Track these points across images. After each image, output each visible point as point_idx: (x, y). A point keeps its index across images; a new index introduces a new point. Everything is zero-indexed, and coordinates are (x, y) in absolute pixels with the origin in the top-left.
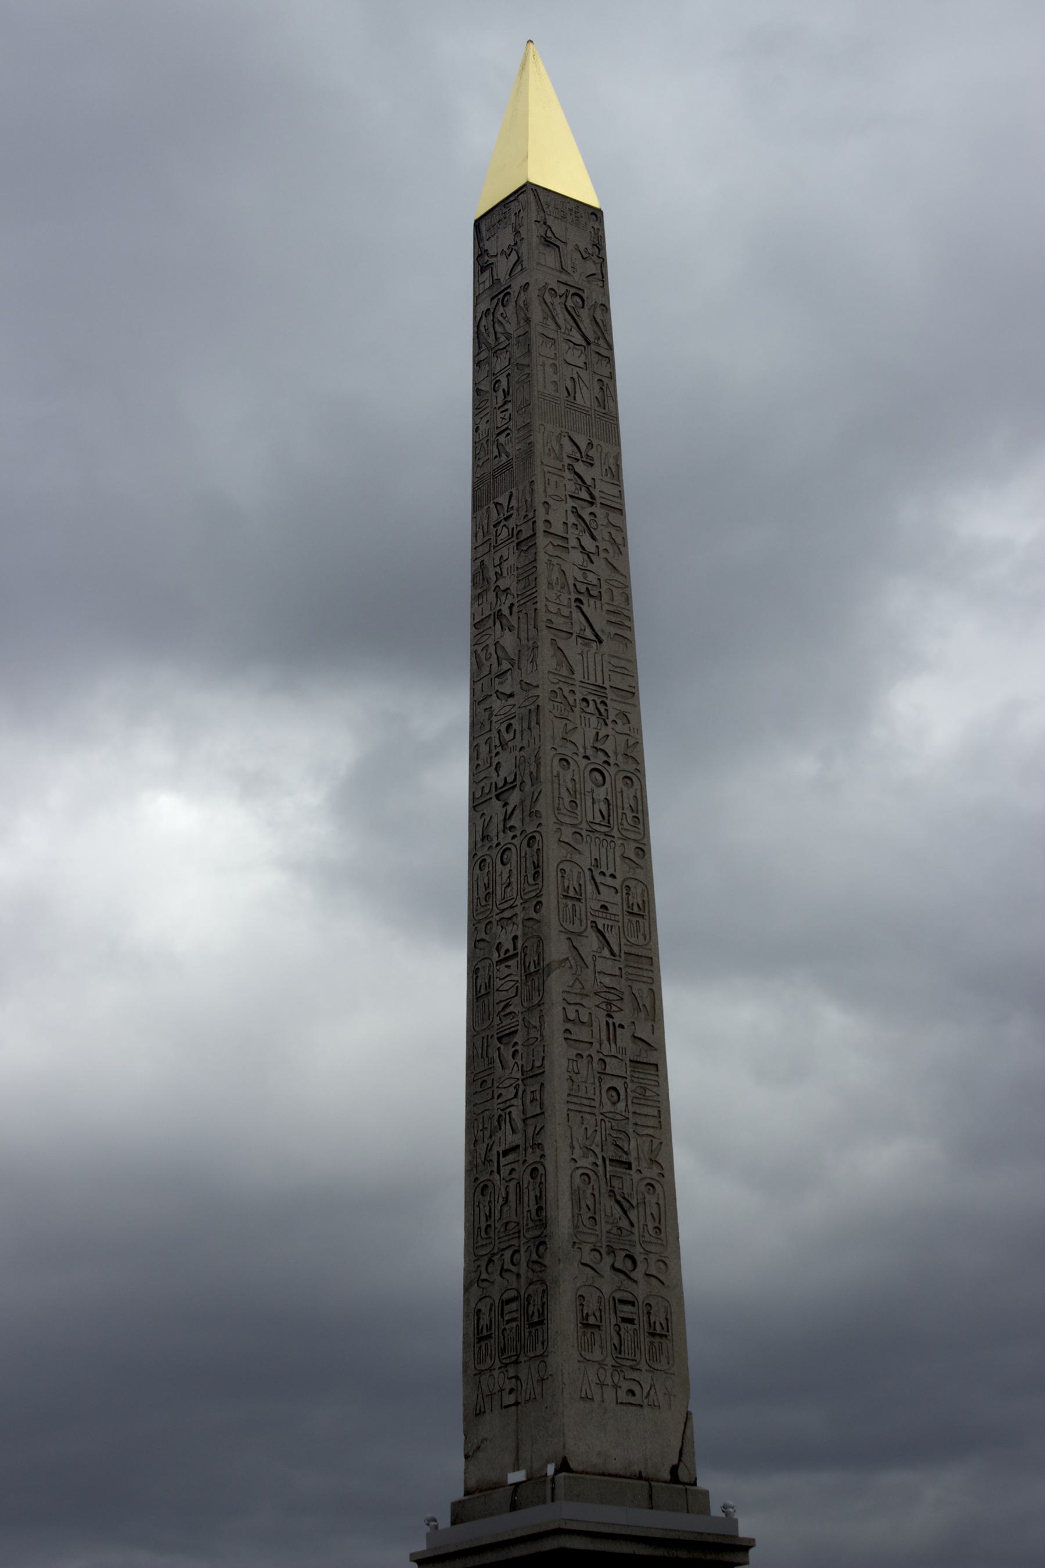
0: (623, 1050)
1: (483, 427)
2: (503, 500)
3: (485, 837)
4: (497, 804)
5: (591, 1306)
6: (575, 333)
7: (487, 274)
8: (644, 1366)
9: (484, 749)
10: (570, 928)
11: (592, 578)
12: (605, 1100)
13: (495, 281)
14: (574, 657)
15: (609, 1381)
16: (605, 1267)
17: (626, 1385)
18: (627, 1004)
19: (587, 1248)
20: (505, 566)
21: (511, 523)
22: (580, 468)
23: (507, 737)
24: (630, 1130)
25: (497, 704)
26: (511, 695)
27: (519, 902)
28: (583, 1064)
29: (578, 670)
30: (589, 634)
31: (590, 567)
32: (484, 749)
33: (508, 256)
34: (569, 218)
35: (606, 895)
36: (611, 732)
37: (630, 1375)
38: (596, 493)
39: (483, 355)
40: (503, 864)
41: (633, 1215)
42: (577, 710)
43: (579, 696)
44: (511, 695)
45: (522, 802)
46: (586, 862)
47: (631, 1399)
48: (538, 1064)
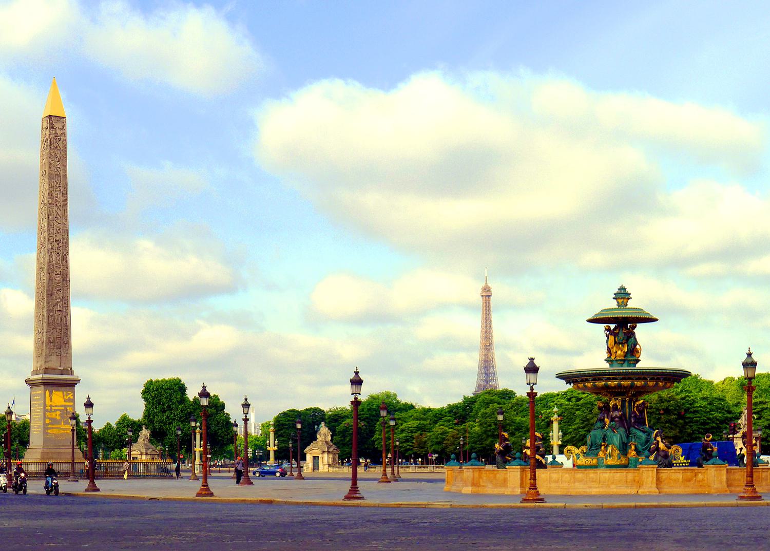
7: (53, 130)
9: (52, 231)
25: (56, 223)
32: (52, 231)
45: (63, 246)
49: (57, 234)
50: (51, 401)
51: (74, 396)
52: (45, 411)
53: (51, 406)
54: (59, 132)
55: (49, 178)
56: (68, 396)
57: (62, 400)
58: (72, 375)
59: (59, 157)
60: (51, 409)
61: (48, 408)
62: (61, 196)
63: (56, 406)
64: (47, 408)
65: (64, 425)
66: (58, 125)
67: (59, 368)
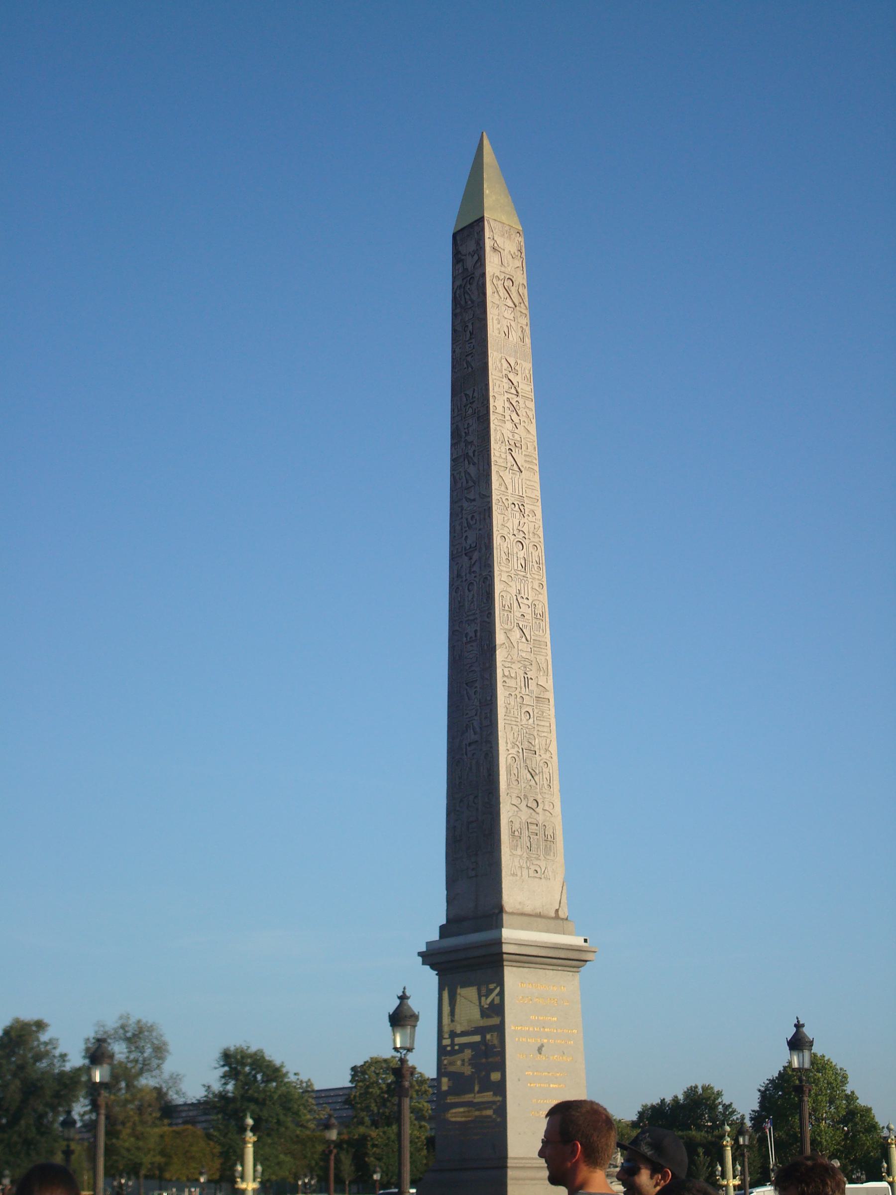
0: (532, 692)
1: (458, 350)
2: (470, 392)
3: (459, 576)
4: (466, 558)
5: (516, 826)
6: (509, 300)
7: (460, 265)
8: (542, 857)
9: (458, 528)
10: (506, 627)
11: (517, 437)
12: (523, 718)
13: (465, 270)
14: (508, 481)
15: (525, 865)
16: (523, 806)
17: (533, 868)
18: (534, 667)
19: (514, 796)
20: (471, 429)
21: (474, 406)
22: (511, 376)
23: (472, 523)
24: (535, 734)
25: (465, 504)
26: (474, 500)
27: (478, 612)
28: (512, 699)
29: (510, 487)
30: (515, 467)
31: (516, 431)
32: (458, 528)
33: (473, 256)
34: (506, 235)
35: (524, 609)
36: (526, 521)
37: (536, 862)
38: (519, 390)
39: (458, 311)
40: (469, 591)
41: (536, 778)
42: (509, 509)
43: (510, 502)
44: (474, 500)
45: (480, 558)
46: (514, 592)
47: (536, 875)
48: (489, 698)
50: (452, 1021)
51: (502, 994)
53: (453, 1035)
60: (453, 1044)
61: (447, 1042)
63: (464, 1034)
65: (479, 1092)
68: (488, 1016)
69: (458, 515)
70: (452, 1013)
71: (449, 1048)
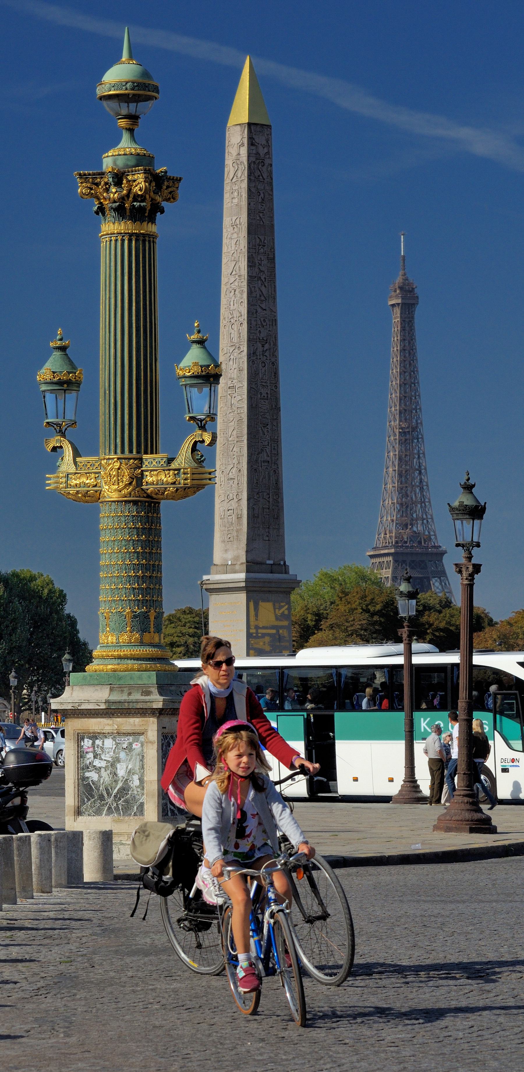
7: (253, 148)
9: (254, 323)
21: (265, 248)
23: (264, 324)
25: (259, 310)
26: (265, 310)
44: (265, 310)
45: (270, 349)
49: (262, 330)
50: (257, 620)
52: (249, 636)
53: (257, 627)
54: (262, 151)
55: (249, 233)
56: (281, 611)
57: (273, 618)
58: (286, 573)
59: (262, 195)
60: (257, 633)
61: (253, 631)
62: (265, 262)
63: (264, 628)
64: (251, 631)
66: (261, 140)
67: (268, 562)
68: (280, 620)
69: (253, 314)
70: (256, 615)
71: (254, 635)
